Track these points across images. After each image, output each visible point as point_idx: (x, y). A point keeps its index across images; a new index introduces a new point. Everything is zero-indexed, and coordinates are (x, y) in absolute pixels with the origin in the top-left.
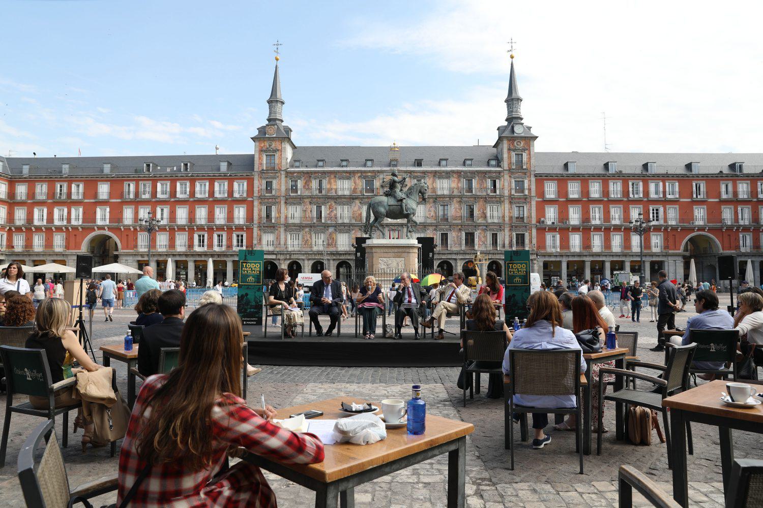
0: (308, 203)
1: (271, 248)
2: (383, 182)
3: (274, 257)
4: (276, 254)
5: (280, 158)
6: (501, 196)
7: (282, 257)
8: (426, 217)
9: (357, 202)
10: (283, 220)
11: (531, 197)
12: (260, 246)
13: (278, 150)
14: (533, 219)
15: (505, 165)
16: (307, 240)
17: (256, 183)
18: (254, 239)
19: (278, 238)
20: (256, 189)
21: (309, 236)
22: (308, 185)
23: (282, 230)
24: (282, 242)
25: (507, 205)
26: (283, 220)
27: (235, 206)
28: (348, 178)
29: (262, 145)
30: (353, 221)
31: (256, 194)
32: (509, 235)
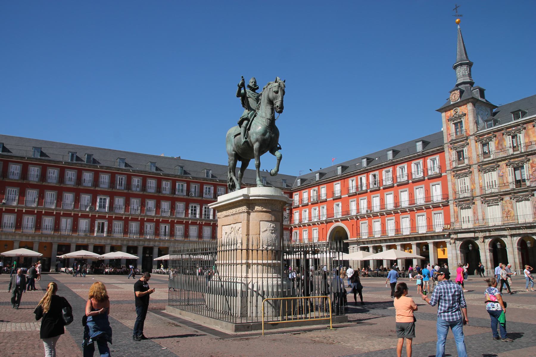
0: (505, 165)
1: (470, 226)
3: (472, 235)
4: (474, 232)
7: (480, 235)
10: (478, 192)
12: (458, 224)
13: (465, 115)
16: (509, 211)
20: (447, 162)
21: (510, 206)
22: (501, 145)
23: (478, 202)
24: (480, 217)
26: (478, 192)
29: (449, 113)
31: (448, 168)
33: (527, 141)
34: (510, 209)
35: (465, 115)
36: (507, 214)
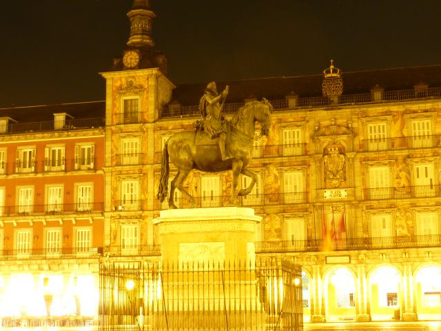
2: (315, 131)
18: (106, 237)
20: (108, 155)
24: (150, 242)
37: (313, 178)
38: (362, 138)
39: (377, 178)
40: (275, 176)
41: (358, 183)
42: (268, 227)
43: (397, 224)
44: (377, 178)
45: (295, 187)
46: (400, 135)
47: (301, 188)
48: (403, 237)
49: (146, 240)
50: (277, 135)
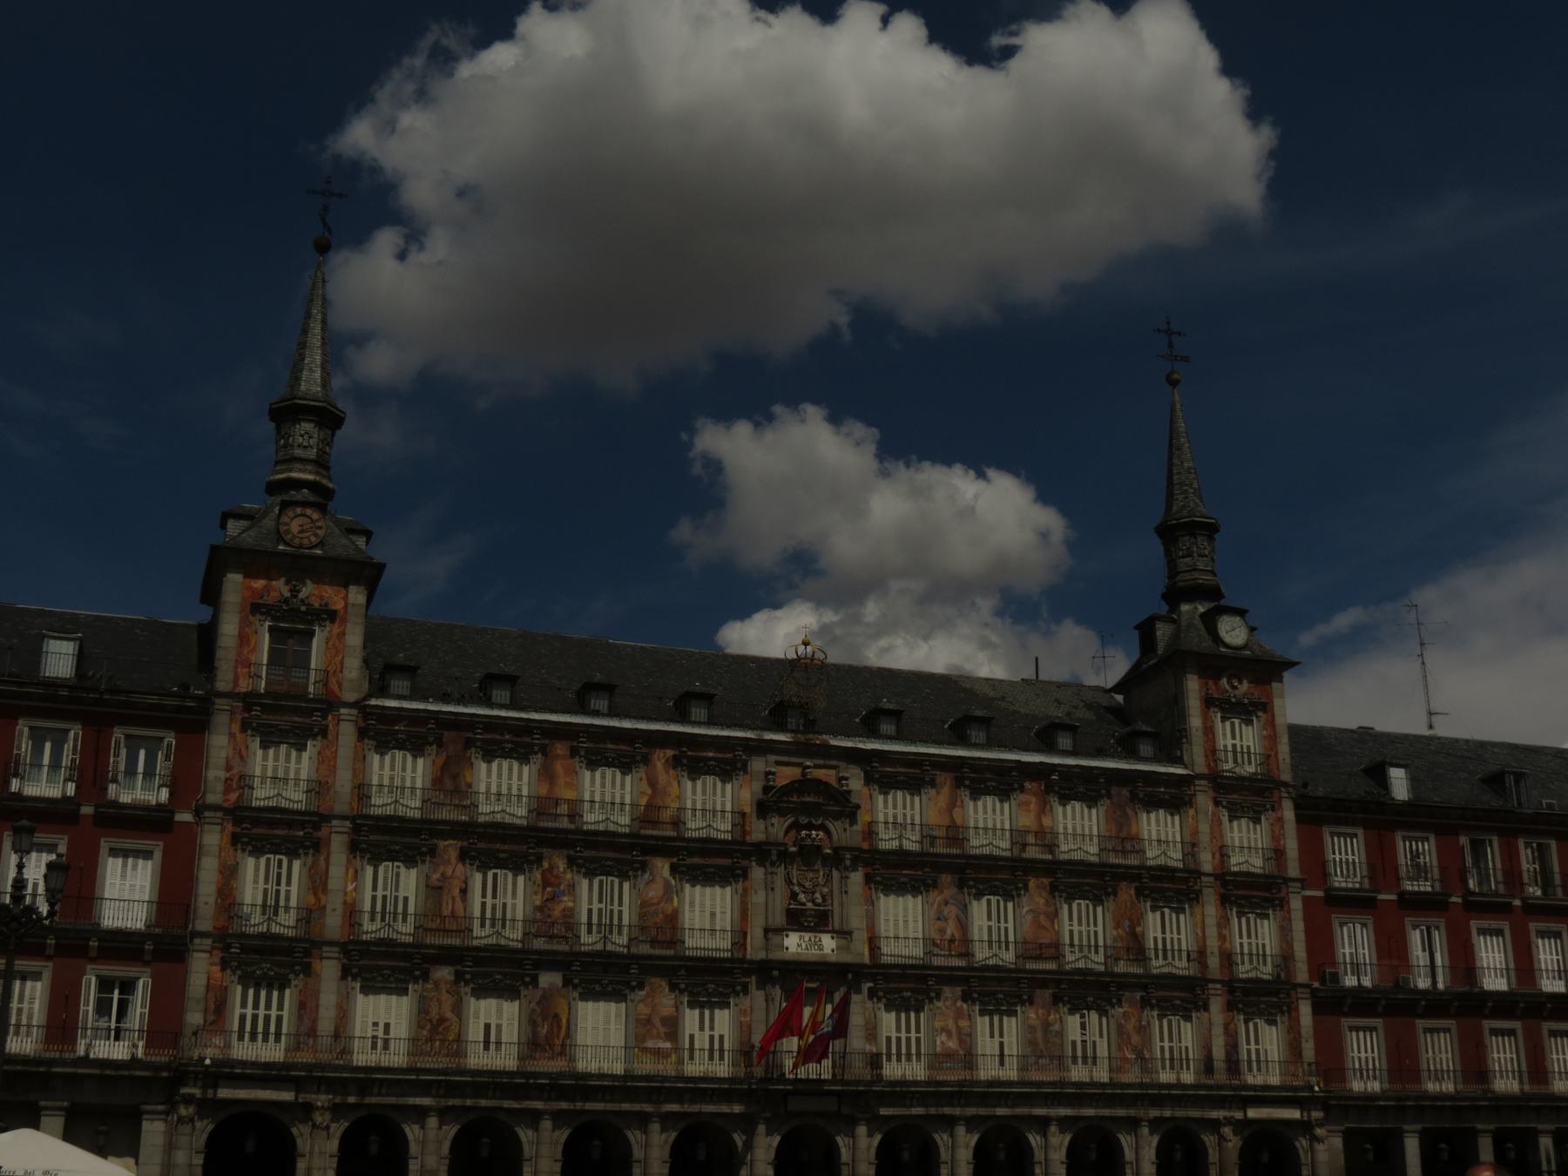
0: (453, 854)
1: (272, 1052)
2: (767, 789)
4: (298, 1084)
5: (336, 647)
6: (1194, 873)
8: (930, 942)
9: (662, 867)
10: (333, 924)
11: (1287, 880)
12: (217, 1041)
13: (332, 616)
14: (1299, 965)
15: (1196, 755)
16: (442, 1020)
17: (219, 744)
19: (306, 1008)
20: (215, 774)
21: (448, 1001)
22: (455, 777)
23: (328, 970)
24: (326, 1025)
25: (1211, 910)
26: (333, 924)
27: (104, 845)
28: (625, 765)
29: (259, 584)
30: (645, 949)
32: (1226, 1026)
33: (544, 791)
34: (449, 1015)
35: (332, 616)
36: (435, 1029)
37: (758, 897)
38: (867, 818)
39: (896, 915)
40: (666, 881)
41: (857, 922)
42: (643, 1009)
43: (938, 1024)
44: (896, 915)
45: (713, 915)
46: (946, 822)
47: (725, 920)
48: (948, 1055)
49: (315, 1021)
50: (675, 784)
